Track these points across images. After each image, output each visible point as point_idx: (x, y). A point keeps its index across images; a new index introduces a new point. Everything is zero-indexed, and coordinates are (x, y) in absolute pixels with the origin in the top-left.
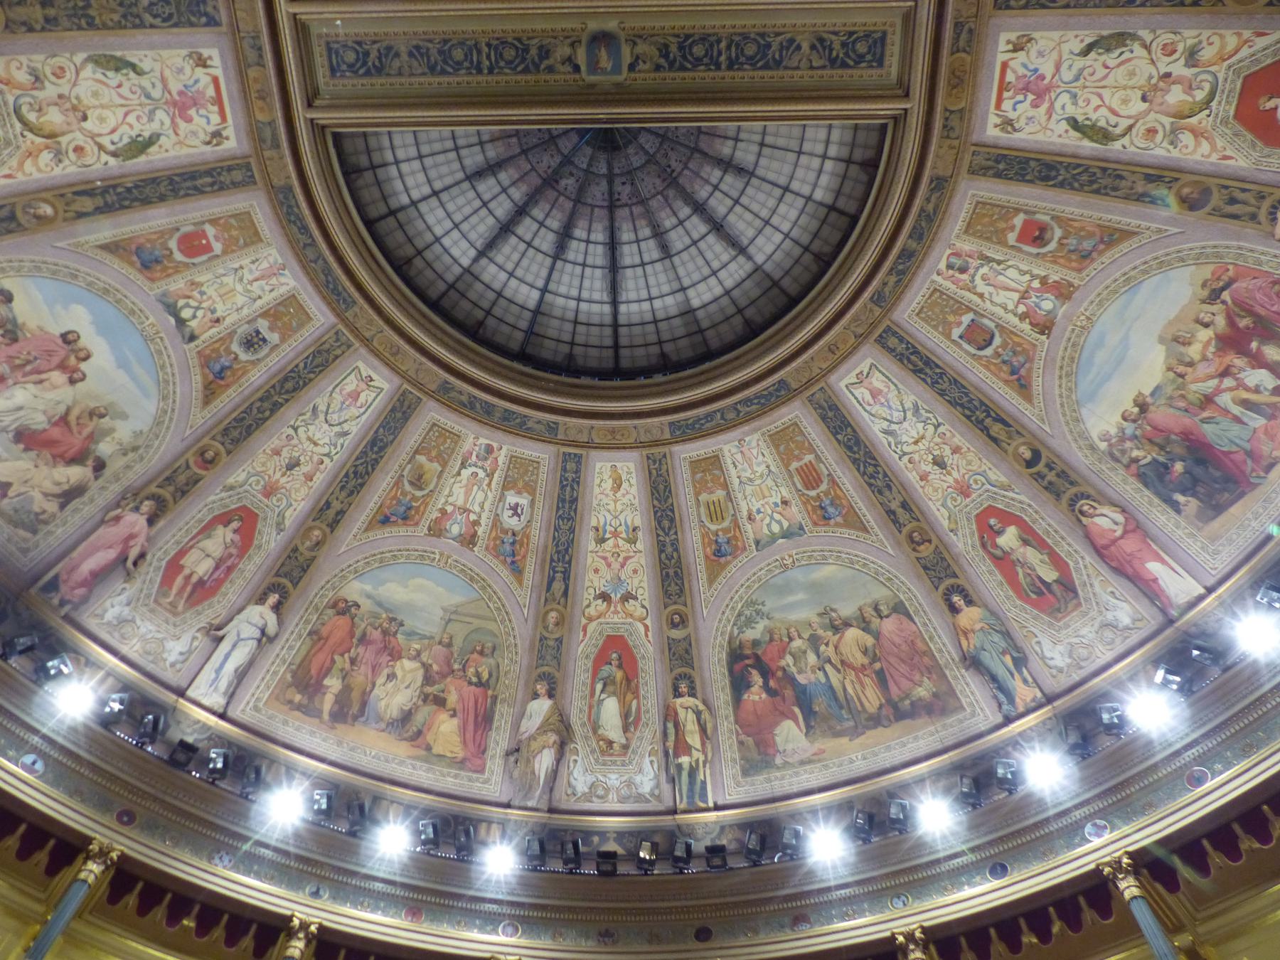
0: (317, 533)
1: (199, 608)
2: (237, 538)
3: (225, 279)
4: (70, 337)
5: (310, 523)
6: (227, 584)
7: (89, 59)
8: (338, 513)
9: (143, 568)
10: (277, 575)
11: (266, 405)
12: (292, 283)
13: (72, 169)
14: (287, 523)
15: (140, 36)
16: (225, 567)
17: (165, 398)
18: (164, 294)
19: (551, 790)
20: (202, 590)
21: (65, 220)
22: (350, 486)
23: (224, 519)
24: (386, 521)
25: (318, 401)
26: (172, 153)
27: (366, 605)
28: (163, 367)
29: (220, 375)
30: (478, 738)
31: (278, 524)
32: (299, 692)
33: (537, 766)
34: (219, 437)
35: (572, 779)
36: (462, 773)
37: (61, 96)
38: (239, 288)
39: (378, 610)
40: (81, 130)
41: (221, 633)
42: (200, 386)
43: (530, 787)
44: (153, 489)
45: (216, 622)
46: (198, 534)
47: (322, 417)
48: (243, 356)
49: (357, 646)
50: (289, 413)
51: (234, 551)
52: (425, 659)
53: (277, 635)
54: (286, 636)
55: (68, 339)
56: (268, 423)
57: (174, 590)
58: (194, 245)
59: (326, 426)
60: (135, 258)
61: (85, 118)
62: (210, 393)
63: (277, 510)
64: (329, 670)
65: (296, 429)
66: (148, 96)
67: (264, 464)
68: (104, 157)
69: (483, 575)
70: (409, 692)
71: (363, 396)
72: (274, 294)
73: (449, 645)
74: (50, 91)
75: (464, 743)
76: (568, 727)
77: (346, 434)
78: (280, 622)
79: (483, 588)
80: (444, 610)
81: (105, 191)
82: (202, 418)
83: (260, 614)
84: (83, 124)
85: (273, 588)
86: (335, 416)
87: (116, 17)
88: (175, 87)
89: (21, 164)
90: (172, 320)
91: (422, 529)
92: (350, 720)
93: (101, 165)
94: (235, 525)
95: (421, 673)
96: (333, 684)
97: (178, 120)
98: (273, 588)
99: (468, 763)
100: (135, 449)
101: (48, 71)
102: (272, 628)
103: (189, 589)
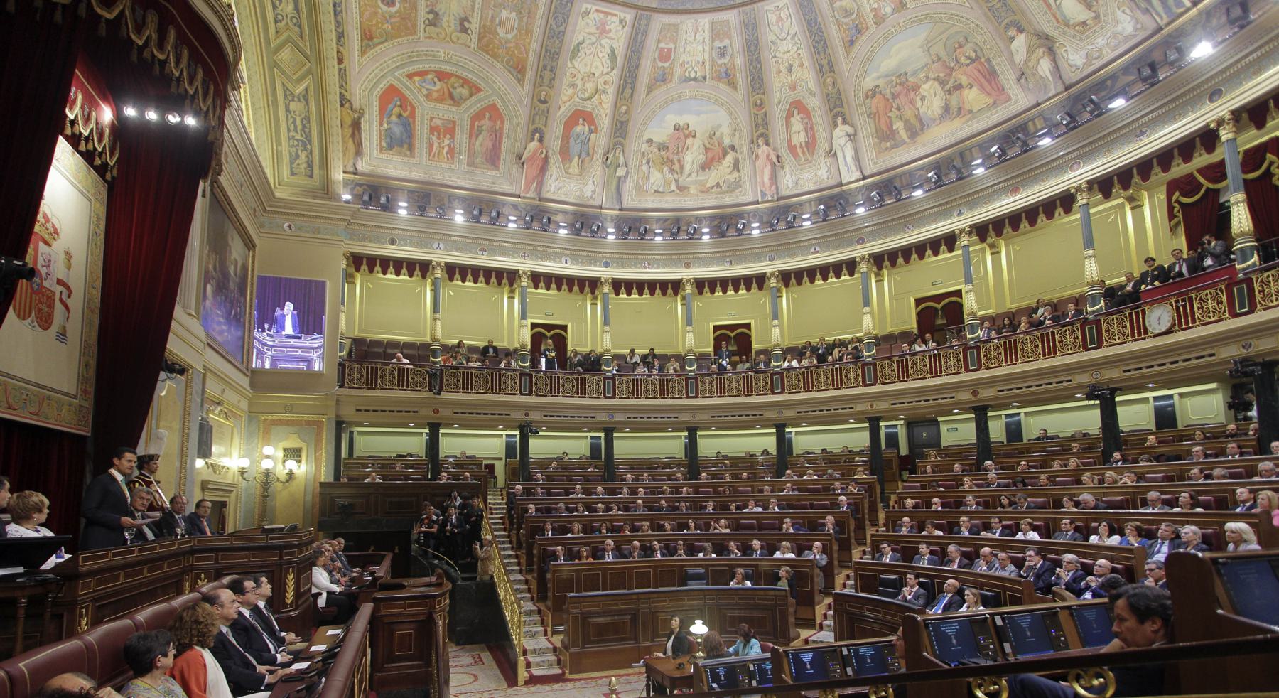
0: (829, 80)
1: (816, 151)
2: (801, 115)
3: (687, 50)
4: (677, 127)
5: (822, 80)
6: (817, 134)
7: (571, 61)
8: (828, 63)
9: (783, 159)
10: (831, 111)
11: (754, 64)
12: (706, 20)
13: (612, 89)
14: (813, 89)
15: (568, 34)
16: (809, 129)
17: (722, 105)
18: (679, 79)
19: (1060, 77)
20: (811, 145)
21: (631, 103)
22: (821, 50)
23: (790, 115)
24: (852, 42)
25: (769, 38)
26: (621, 45)
27: (881, 82)
28: (709, 98)
29: (728, 75)
30: (995, 86)
31: (811, 93)
32: (887, 142)
33: (1041, 73)
34: (754, 94)
35: (1071, 62)
36: (999, 108)
37: (582, 80)
38: (694, 45)
39: (888, 79)
40: (598, 78)
41: (833, 152)
42: (727, 87)
43: (1045, 87)
44: (756, 135)
45: (827, 149)
46: (787, 128)
47: (779, 41)
48: (726, 61)
49: (894, 101)
50: (765, 55)
51: (806, 120)
52: (933, 77)
53: (855, 131)
54: (860, 127)
55: (677, 128)
56: (763, 68)
57: (801, 156)
58: (665, 56)
59: (784, 42)
60: (658, 83)
61: (594, 74)
62: (732, 85)
63: (804, 90)
64: (891, 123)
65: (775, 56)
66: (594, 43)
67: (780, 81)
68: (612, 74)
69: (925, 13)
70: (938, 96)
71: (783, 15)
72: (706, 32)
73: (939, 59)
74: (579, 83)
75: (989, 94)
76: (1048, 38)
77: (795, 34)
78: (852, 126)
79: (932, 18)
80: (921, 47)
81: (626, 81)
82: (741, 96)
83: (841, 130)
84: (597, 75)
85: (835, 117)
86: (783, 34)
87: (557, 42)
88: (593, 30)
89: (603, 108)
90: (692, 82)
91: (873, 27)
92: (920, 133)
93: (614, 77)
94: (796, 112)
95: (936, 84)
96: (898, 125)
97: (608, 35)
98: (835, 117)
99: (998, 102)
100: (735, 130)
101: (571, 80)
102: (850, 130)
103: (805, 149)
